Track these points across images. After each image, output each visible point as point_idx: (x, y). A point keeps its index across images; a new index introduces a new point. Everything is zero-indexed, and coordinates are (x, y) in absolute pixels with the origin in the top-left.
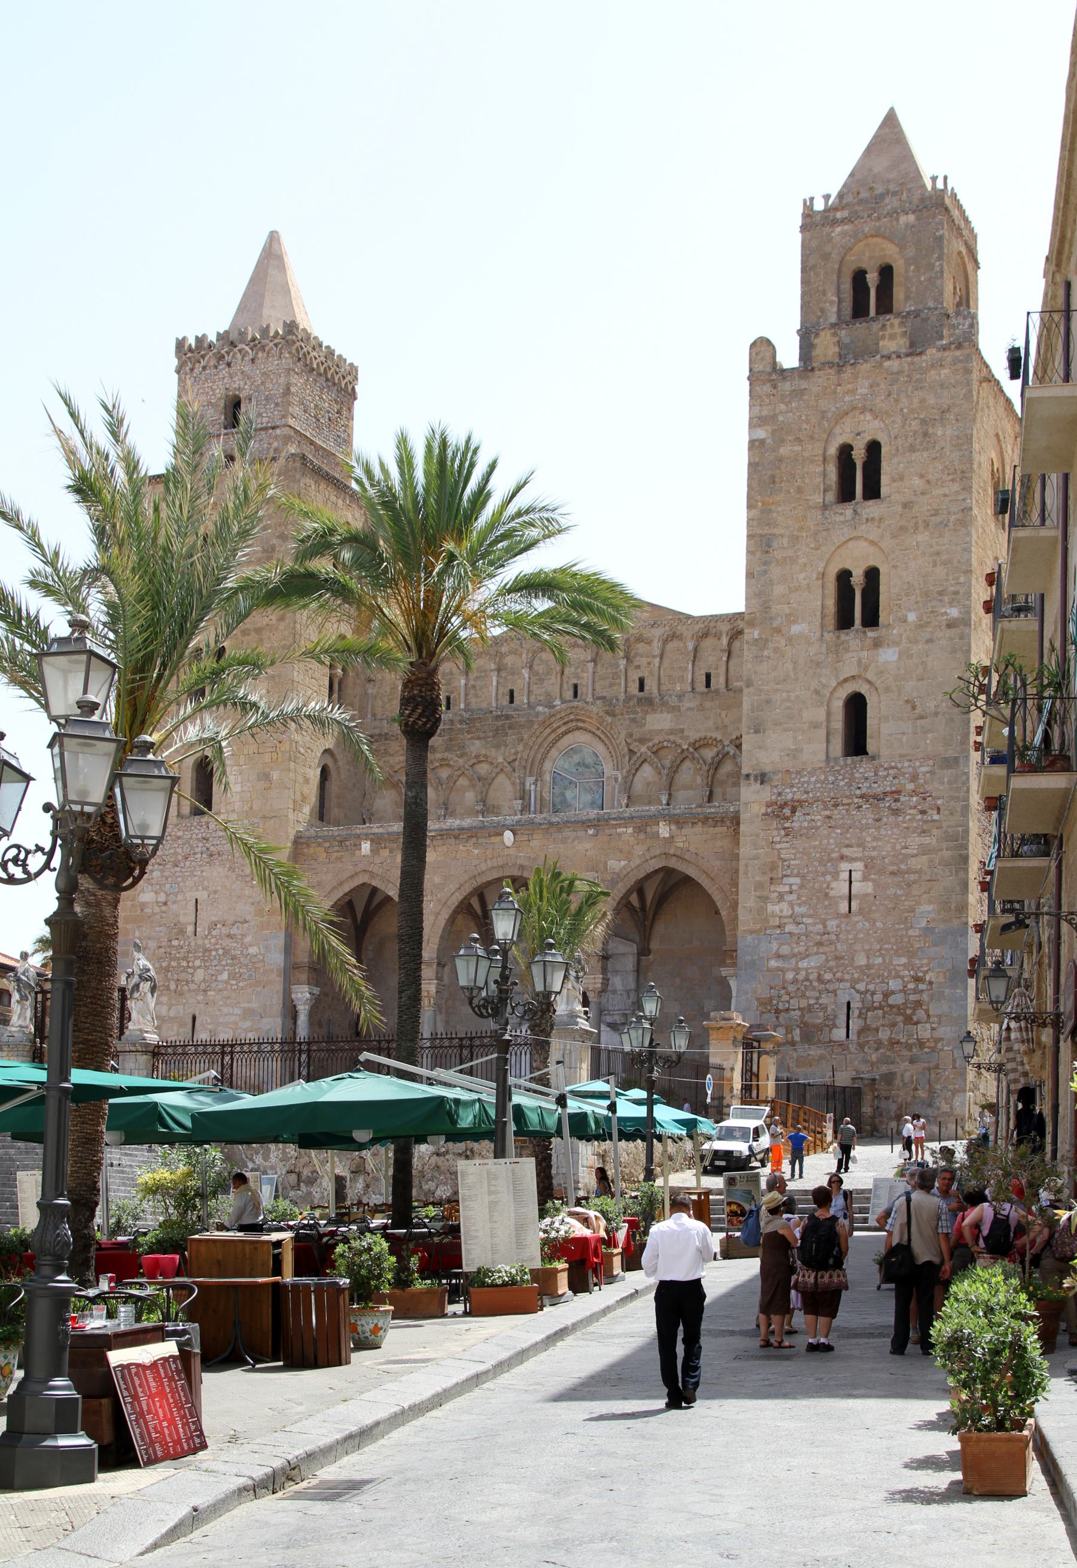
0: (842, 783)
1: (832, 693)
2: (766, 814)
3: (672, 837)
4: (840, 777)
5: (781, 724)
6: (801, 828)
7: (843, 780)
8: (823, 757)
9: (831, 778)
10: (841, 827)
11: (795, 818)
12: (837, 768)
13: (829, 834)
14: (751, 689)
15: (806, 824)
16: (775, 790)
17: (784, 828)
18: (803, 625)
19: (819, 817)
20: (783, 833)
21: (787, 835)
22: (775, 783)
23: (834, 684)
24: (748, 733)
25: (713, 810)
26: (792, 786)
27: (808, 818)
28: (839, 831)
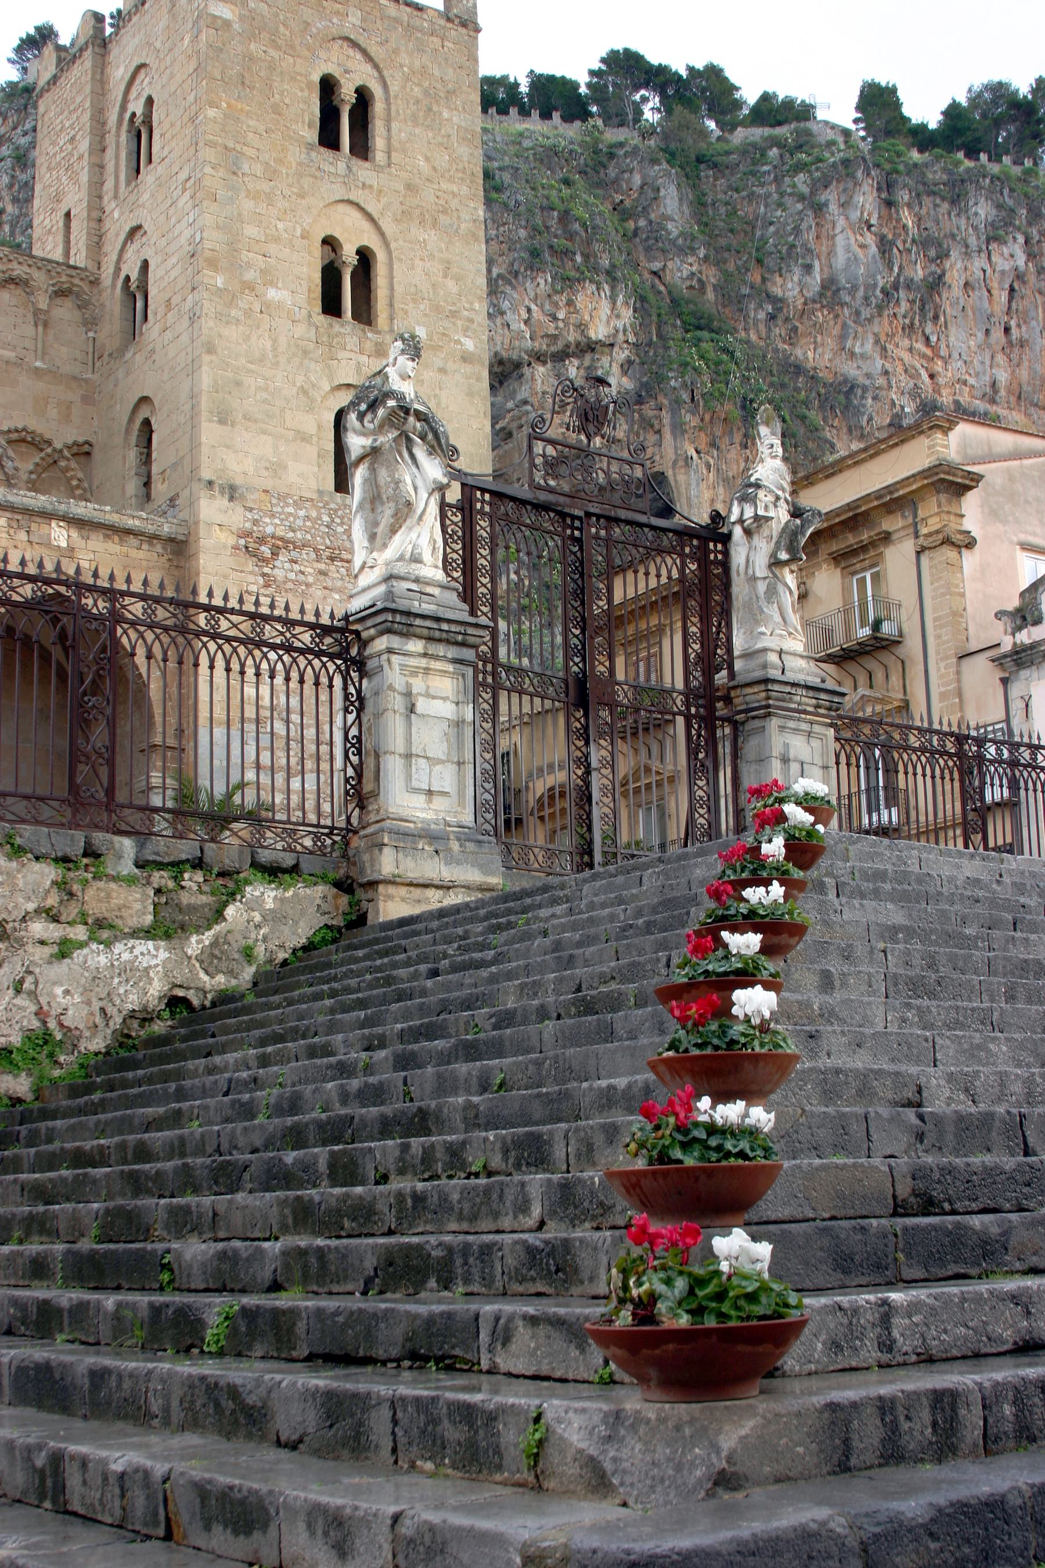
0: (340, 529)
1: (324, 398)
2: (236, 548)
3: (71, 549)
4: (338, 520)
5: (256, 421)
6: (287, 580)
7: (342, 524)
8: (314, 485)
9: (326, 518)
10: (340, 591)
11: (277, 563)
12: (332, 506)
13: (325, 598)
14: (214, 357)
15: (292, 576)
16: (249, 515)
17: (264, 575)
18: (285, 293)
19: (311, 571)
20: (261, 581)
21: (267, 586)
22: (251, 505)
23: (327, 388)
24: (211, 421)
25: (137, 523)
26: (273, 516)
27: (296, 567)
28: (337, 596)
